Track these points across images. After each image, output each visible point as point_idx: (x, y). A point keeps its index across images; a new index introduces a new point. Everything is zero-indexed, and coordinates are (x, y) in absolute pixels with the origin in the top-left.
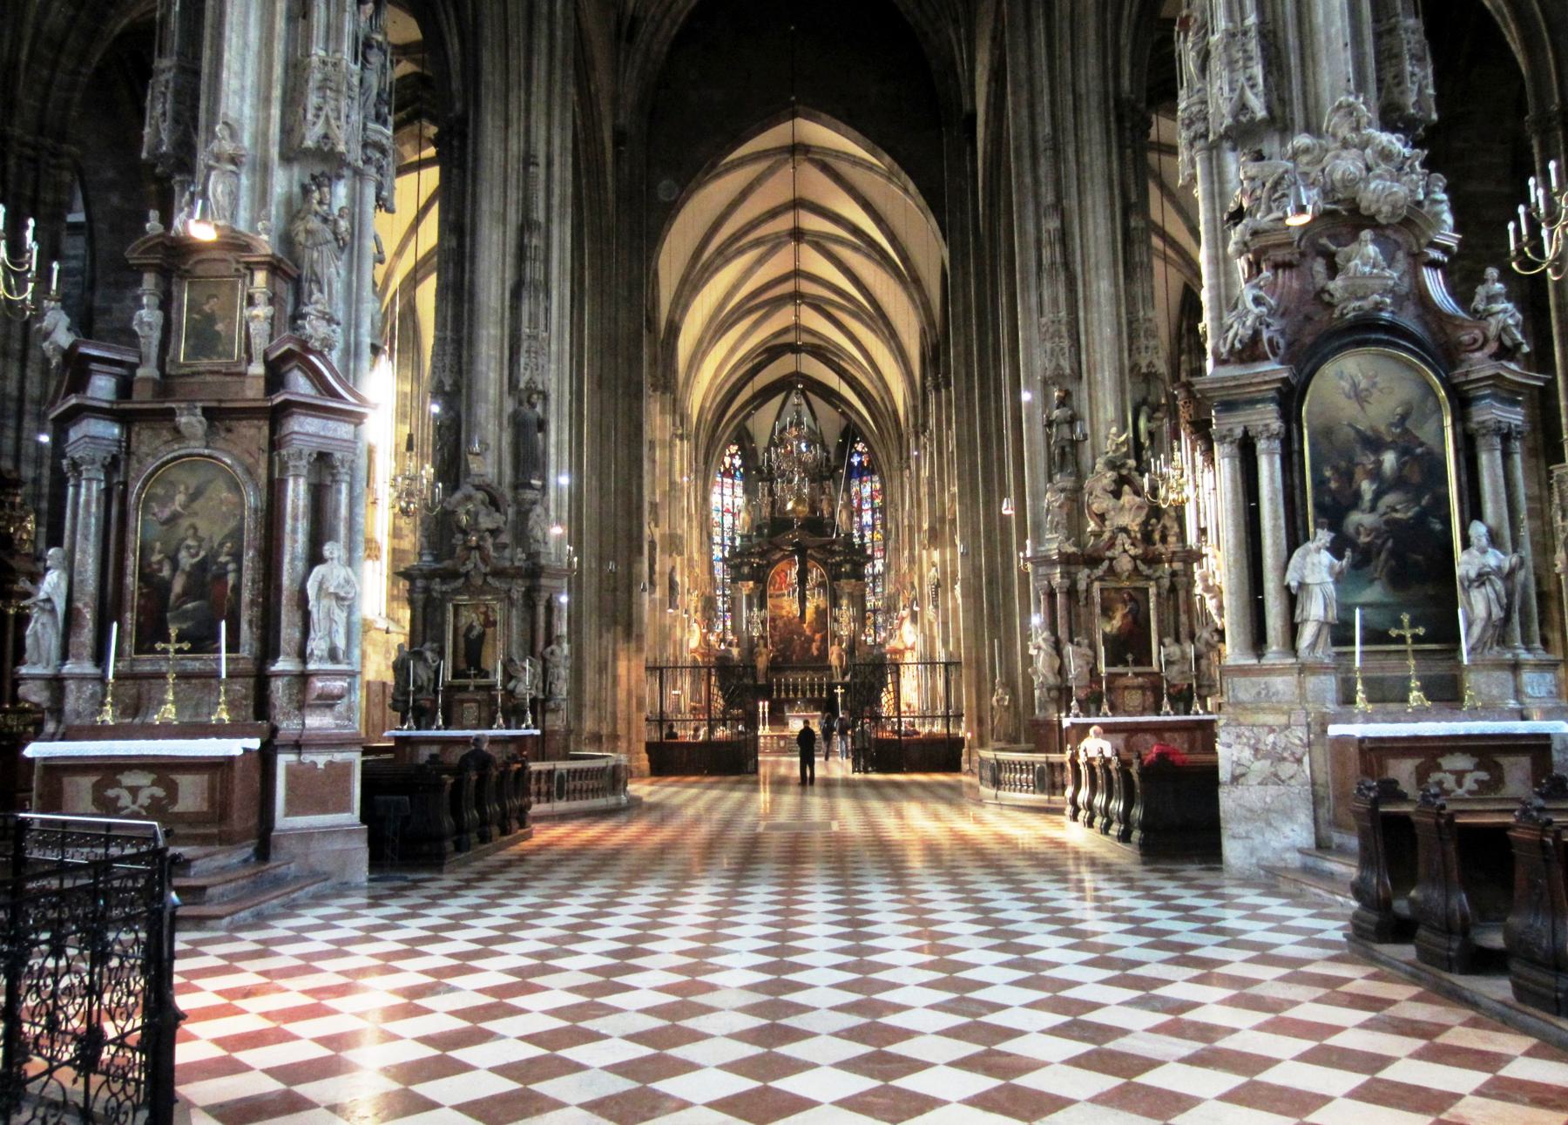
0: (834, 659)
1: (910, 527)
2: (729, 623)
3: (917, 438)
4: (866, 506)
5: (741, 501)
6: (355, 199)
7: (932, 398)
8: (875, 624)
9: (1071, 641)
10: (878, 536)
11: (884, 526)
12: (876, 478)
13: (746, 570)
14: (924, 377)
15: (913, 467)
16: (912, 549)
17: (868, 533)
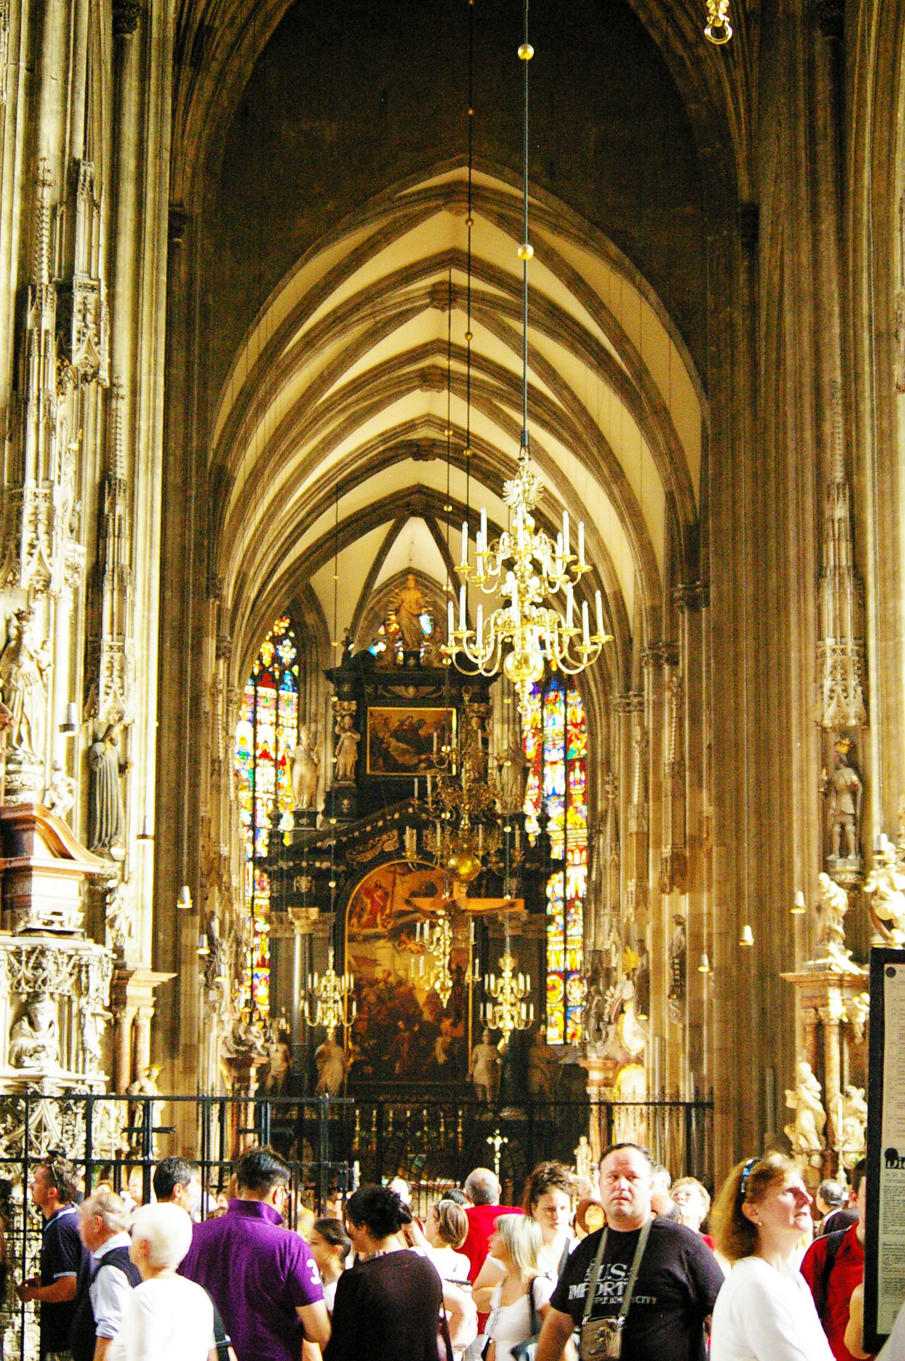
0: (480, 1073)
1: (643, 839)
2: (263, 992)
3: (658, 668)
4: (554, 754)
5: (289, 736)
6: (50, 623)
7: (684, 619)
8: (565, 999)
9: (842, 1091)
10: (579, 816)
11: (590, 798)
12: (575, 697)
13: (303, 883)
14: (672, 583)
15: (649, 722)
16: (642, 877)
17: (555, 810)
